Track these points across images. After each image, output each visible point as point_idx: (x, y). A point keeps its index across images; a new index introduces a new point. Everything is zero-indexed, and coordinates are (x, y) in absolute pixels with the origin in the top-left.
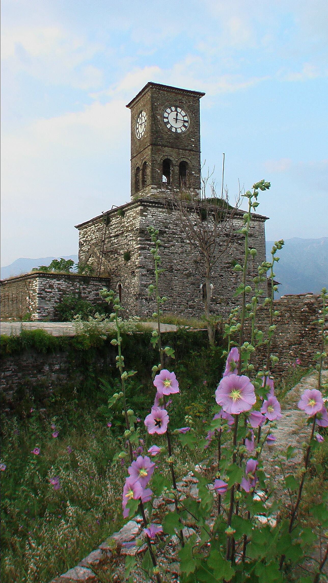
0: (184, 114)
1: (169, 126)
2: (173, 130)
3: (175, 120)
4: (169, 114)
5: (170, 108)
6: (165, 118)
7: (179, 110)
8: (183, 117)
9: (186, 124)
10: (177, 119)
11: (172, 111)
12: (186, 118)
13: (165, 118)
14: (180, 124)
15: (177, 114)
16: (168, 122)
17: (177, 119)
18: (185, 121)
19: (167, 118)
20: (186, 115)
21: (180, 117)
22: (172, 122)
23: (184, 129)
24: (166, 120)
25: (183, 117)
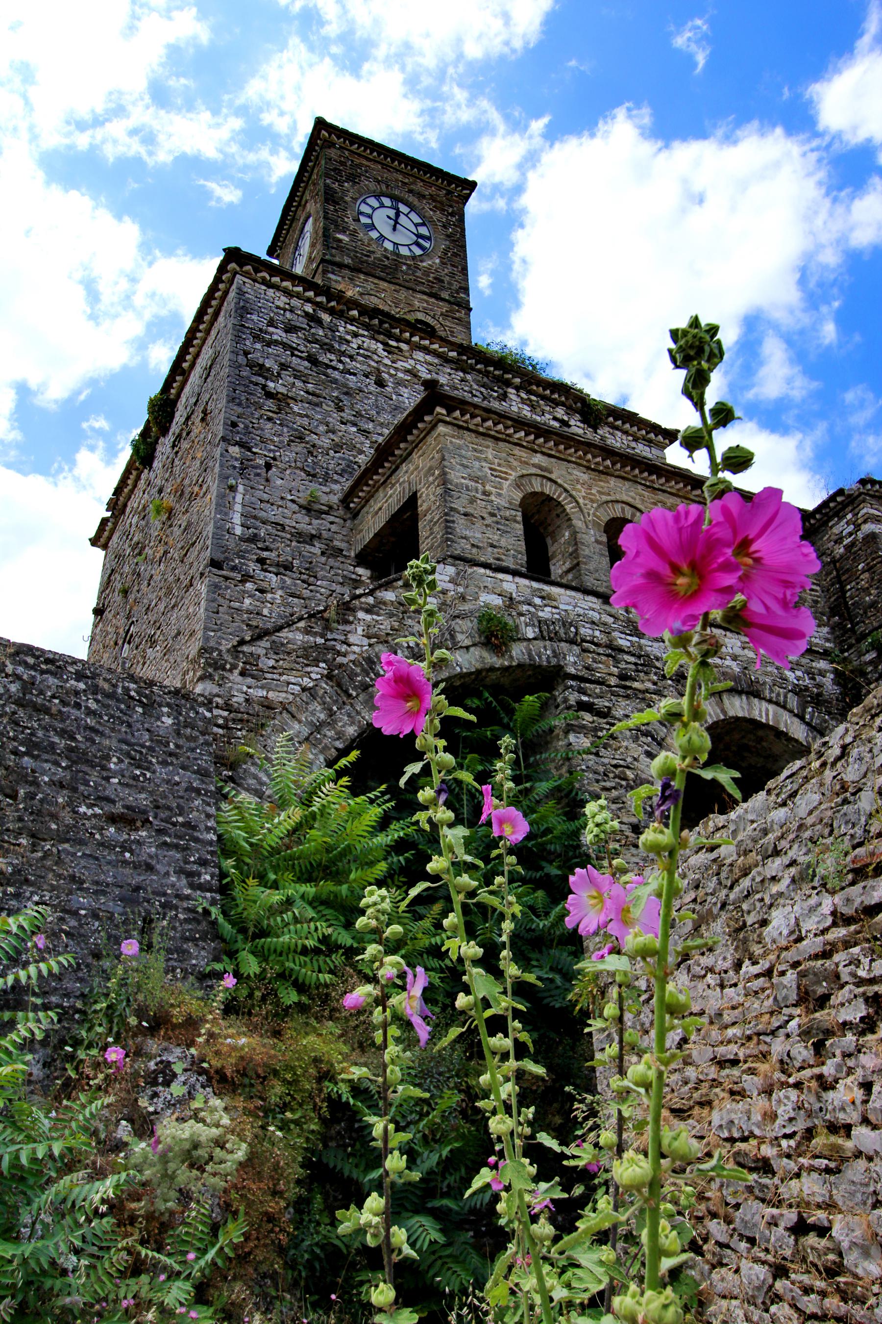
1: (374, 235)
3: (391, 227)
4: (374, 209)
5: (377, 197)
6: (362, 213)
7: (403, 208)
8: (416, 225)
10: (396, 222)
12: (423, 231)
14: (404, 237)
15: (398, 214)
16: (372, 227)
18: (419, 236)
20: (423, 224)
23: (418, 252)
24: (364, 220)
25: (416, 225)
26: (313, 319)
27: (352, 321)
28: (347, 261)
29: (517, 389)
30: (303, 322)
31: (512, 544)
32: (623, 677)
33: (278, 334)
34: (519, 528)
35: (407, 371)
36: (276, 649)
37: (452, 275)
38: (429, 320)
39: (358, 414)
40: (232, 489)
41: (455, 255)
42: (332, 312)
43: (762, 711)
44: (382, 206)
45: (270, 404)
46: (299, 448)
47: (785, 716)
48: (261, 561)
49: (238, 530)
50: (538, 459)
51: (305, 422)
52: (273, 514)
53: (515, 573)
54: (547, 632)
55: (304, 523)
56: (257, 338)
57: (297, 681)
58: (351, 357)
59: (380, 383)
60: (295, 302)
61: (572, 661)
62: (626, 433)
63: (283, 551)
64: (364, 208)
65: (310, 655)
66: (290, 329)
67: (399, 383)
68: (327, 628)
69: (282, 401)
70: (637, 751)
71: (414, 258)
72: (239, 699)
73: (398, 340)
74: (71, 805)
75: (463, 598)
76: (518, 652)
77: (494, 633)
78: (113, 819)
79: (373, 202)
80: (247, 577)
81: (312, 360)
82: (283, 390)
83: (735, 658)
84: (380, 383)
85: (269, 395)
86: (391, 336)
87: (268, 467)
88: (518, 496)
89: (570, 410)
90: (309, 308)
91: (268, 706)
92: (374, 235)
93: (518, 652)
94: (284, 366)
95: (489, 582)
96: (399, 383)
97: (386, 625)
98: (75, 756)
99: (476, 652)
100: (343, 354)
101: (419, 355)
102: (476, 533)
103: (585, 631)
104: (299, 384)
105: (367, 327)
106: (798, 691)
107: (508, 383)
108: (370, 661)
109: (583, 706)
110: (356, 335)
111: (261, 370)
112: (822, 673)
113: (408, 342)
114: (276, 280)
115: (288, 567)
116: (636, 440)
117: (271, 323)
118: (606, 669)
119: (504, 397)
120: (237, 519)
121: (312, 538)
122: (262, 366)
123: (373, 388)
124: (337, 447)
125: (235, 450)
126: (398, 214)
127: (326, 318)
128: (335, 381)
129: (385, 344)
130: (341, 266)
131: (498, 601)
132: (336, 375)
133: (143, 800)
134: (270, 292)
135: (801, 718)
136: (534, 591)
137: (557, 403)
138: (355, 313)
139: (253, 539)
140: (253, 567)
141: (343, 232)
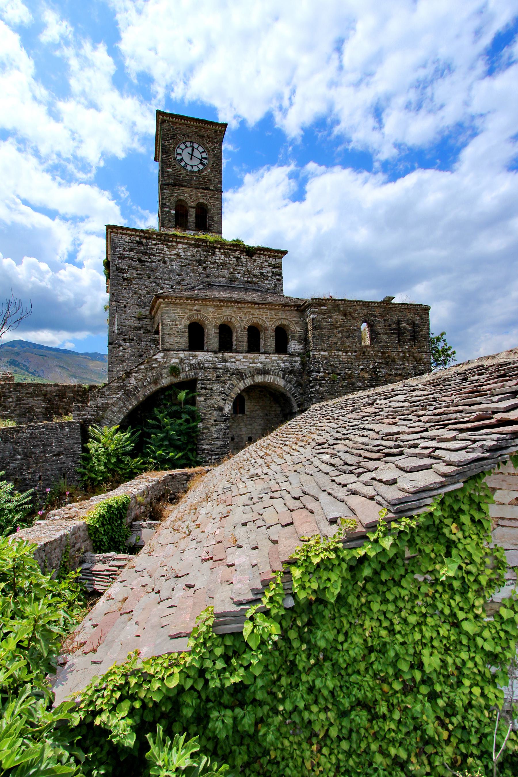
0: (201, 150)
1: (183, 164)
2: (189, 168)
3: (190, 157)
5: (184, 143)
6: (177, 154)
7: (196, 146)
9: (205, 162)
10: (192, 155)
11: (186, 147)
12: (204, 155)
13: (177, 154)
14: (195, 162)
15: (193, 151)
16: (182, 160)
17: (192, 155)
19: (181, 155)
21: (196, 153)
22: (186, 158)
23: (201, 167)
24: (179, 157)
26: (140, 243)
27: (154, 239)
28: (171, 181)
29: (220, 249)
30: (135, 246)
31: (184, 340)
32: (218, 377)
33: (127, 254)
34: (187, 335)
35: (175, 254)
36: (110, 389)
37: (215, 176)
38: (205, 202)
39: (157, 278)
40: (114, 318)
41: (217, 165)
42: (146, 238)
43: (269, 379)
44: (186, 147)
45: (125, 283)
46: (135, 297)
47: (278, 379)
48: (124, 340)
49: (116, 331)
50: (196, 307)
51: (137, 286)
52: (128, 323)
53: (184, 350)
54: (193, 367)
55: (137, 324)
56: (120, 258)
57: (115, 397)
58: (154, 255)
59: (165, 262)
60: (133, 238)
61: (201, 375)
62: (265, 255)
63: (131, 335)
64: (179, 151)
65: (119, 389)
66: (131, 250)
67: (172, 260)
68: (124, 380)
69: (129, 280)
70: (219, 399)
71: (200, 171)
72: (100, 404)
73: (172, 242)
74: (45, 455)
75: (166, 362)
76: (182, 376)
77: (175, 371)
78: (54, 455)
79: (183, 146)
80: (120, 346)
81: (140, 261)
82: (129, 276)
83: (261, 363)
84: (165, 262)
85: (124, 279)
86: (169, 241)
87: (125, 306)
88: (188, 323)
89: (241, 252)
90: (138, 239)
91: (107, 404)
92: (183, 164)
93: (182, 376)
94: (129, 266)
95: (175, 356)
96: (172, 260)
97: (141, 375)
98: (44, 445)
99: (169, 378)
100: (151, 254)
101: (180, 246)
102: (172, 340)
103: (206, 365)
104: (135, 272)
105: (160, 240)
106: (284, 370)
107: (216, 248)
108: (136, 387)
109: (202, 388)
110: (155, 245)
111: (122, 271)
112: (296, 362)
113: (176, 242)
114: (125, 232)
115: (133, 340)
116: (269, 257)
117: (124, 250)
118: (212, 375)
119: (214, 254)
120: (116, 327)
121: (139, 329)
122: (122, 269)
123: (162, 265)
124: (148, 293)
125: (114, 303)
126: (193, 151)
127: (144, 241)
128: (148, 267)
129: (167, 245)
130: (168, 185)
131: (177, 361)
132: (148, 264)
133: (62, 449)
134: (124, 237)
135: (283, 378)
136: (190, 355)
137: (236, 251)
138: (155, 236)
139: (121, 333)
140: (122, 342)
141: (169, 167)
